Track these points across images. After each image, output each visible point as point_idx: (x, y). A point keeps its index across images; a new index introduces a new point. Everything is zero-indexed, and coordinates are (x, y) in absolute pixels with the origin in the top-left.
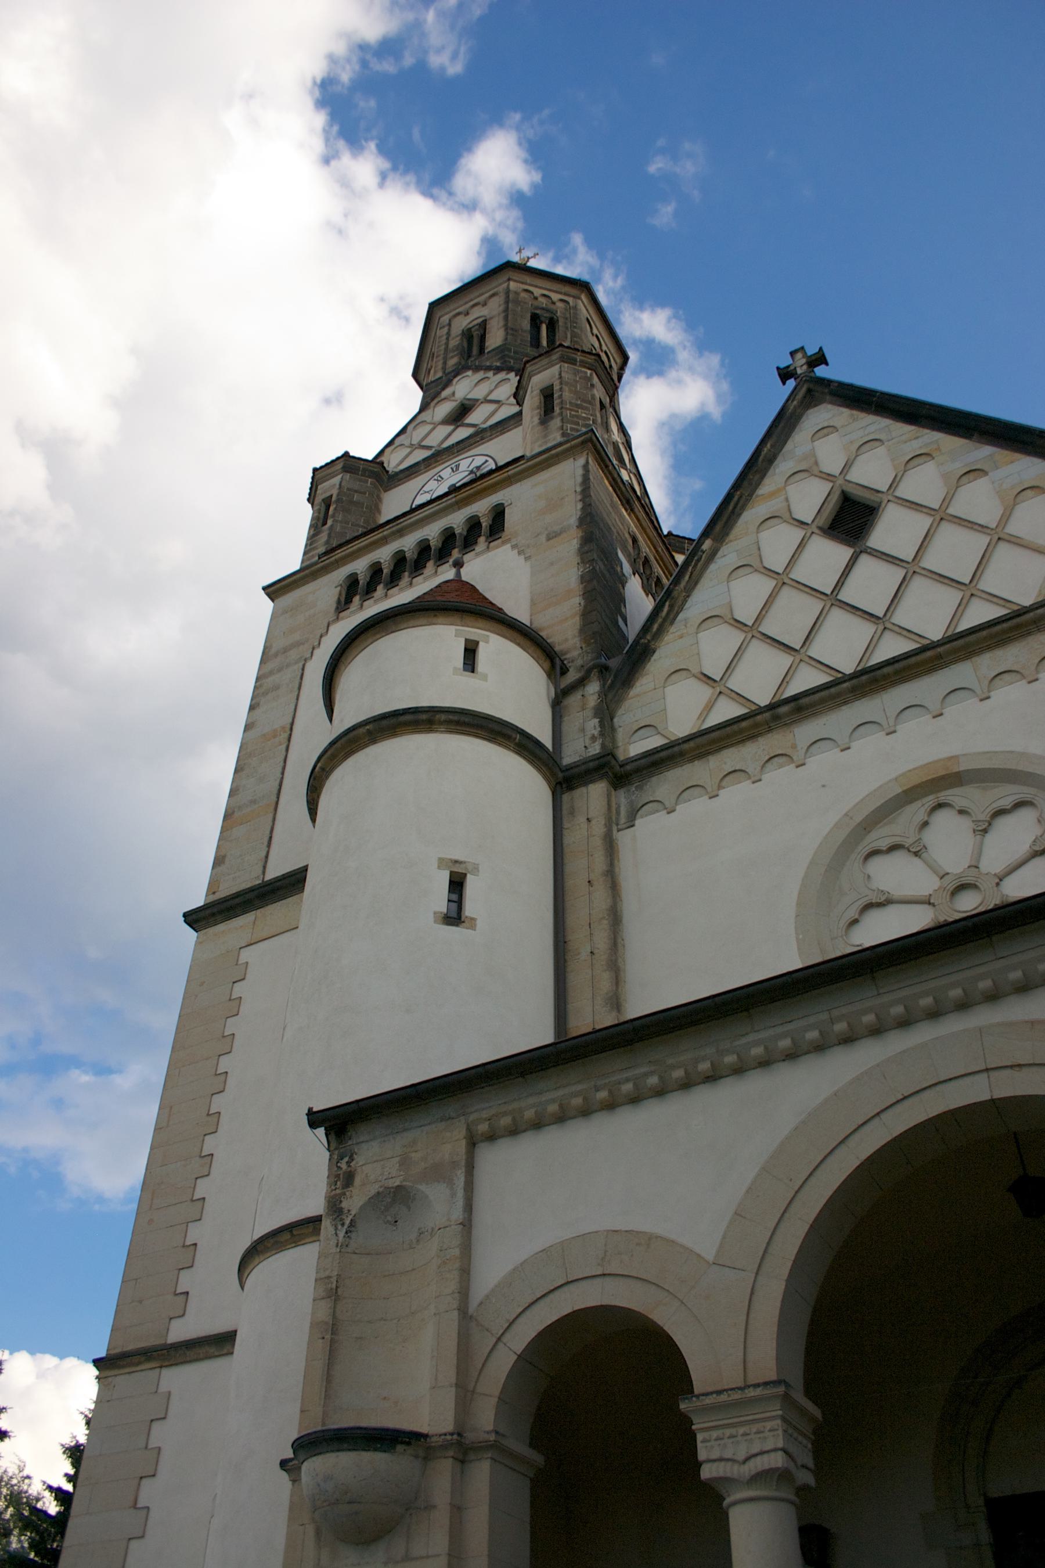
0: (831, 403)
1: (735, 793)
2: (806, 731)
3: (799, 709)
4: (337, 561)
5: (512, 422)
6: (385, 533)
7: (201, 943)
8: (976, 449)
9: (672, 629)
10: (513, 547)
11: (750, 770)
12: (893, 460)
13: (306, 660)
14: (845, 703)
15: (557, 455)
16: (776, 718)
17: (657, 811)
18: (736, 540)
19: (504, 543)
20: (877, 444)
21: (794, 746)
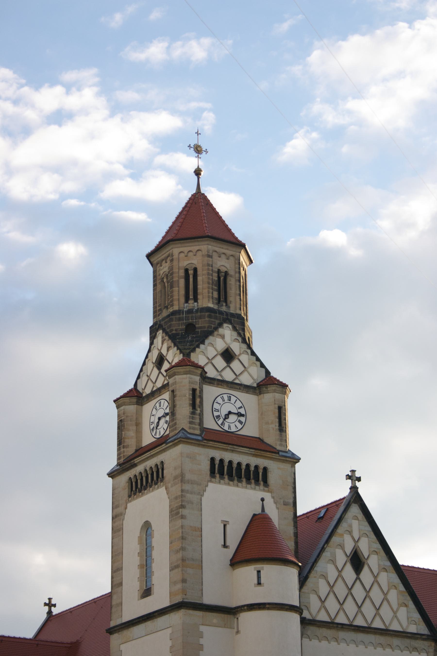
0: (359, 506)
1: (324, 643)
2: (342, 634)
3: (342, 628)
4: (209, 446)
5: (251, 390)
6: (229, 448)
7: (185, 615)
8: (387, 561)
9: (313, 572)
10: (273, 497)
11: (329, 638)
12: (369, 548)
13: (201, 495)
14: (350, 631)
15: (287, 461)
16: (337, 627)
17: (307, 638)
18: (330, 547)
19: (268, 491)
20: (366, 536)
21: (338, 638)
